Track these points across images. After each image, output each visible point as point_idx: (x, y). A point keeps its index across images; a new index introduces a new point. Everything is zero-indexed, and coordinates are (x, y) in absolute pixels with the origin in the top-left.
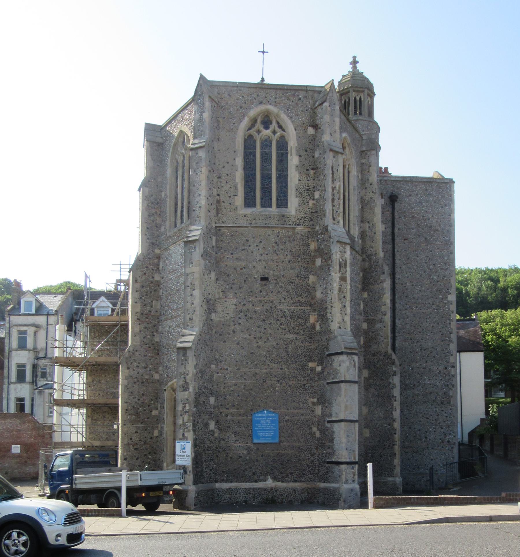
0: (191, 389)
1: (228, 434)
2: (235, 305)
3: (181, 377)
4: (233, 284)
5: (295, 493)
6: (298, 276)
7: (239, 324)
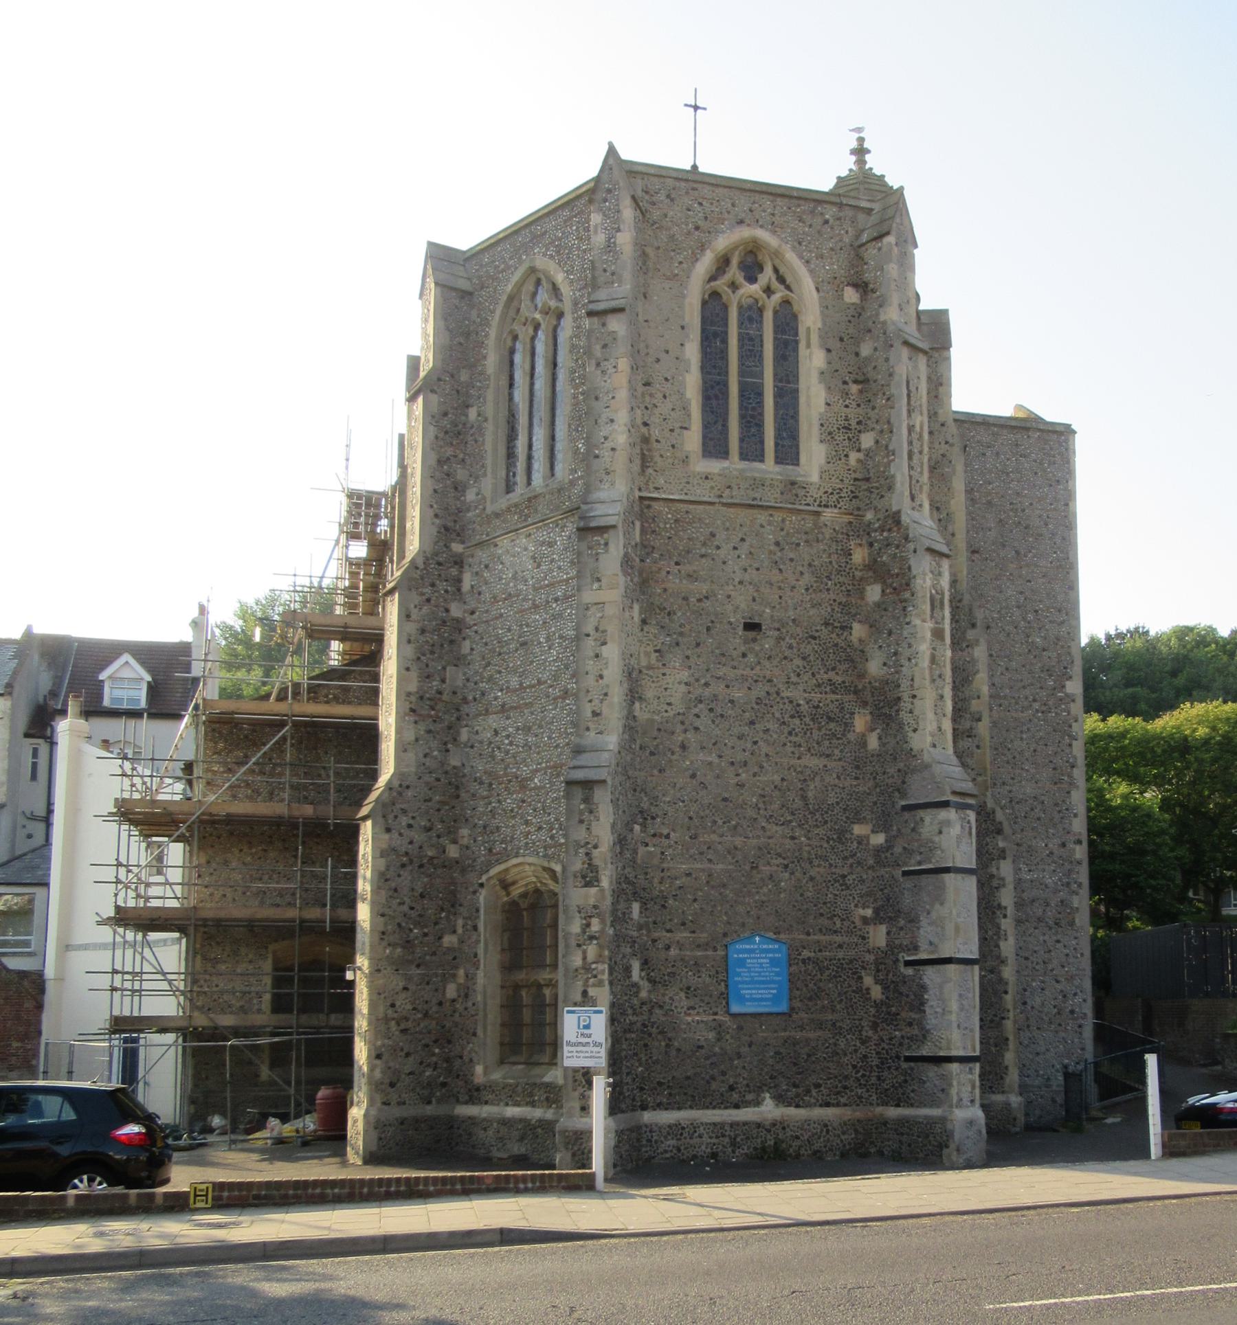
0: (605, 883)
1: (670, 993)
2: (686, 684)
3: (576, 853)
4: (681, 634)
5: (828, 1131)
6: (826, 624)
7: (696, 729)
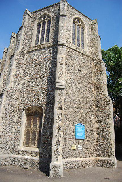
0: (63, 109)
